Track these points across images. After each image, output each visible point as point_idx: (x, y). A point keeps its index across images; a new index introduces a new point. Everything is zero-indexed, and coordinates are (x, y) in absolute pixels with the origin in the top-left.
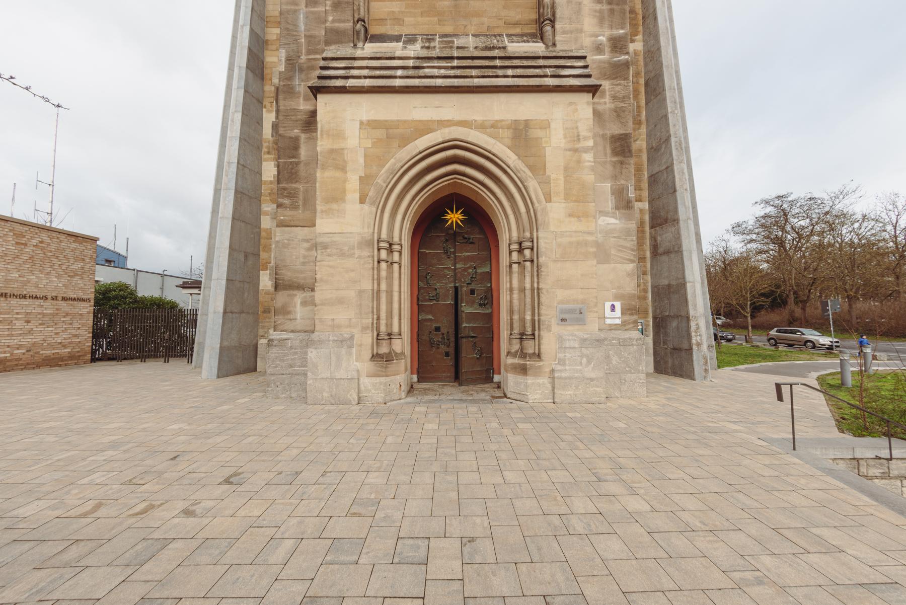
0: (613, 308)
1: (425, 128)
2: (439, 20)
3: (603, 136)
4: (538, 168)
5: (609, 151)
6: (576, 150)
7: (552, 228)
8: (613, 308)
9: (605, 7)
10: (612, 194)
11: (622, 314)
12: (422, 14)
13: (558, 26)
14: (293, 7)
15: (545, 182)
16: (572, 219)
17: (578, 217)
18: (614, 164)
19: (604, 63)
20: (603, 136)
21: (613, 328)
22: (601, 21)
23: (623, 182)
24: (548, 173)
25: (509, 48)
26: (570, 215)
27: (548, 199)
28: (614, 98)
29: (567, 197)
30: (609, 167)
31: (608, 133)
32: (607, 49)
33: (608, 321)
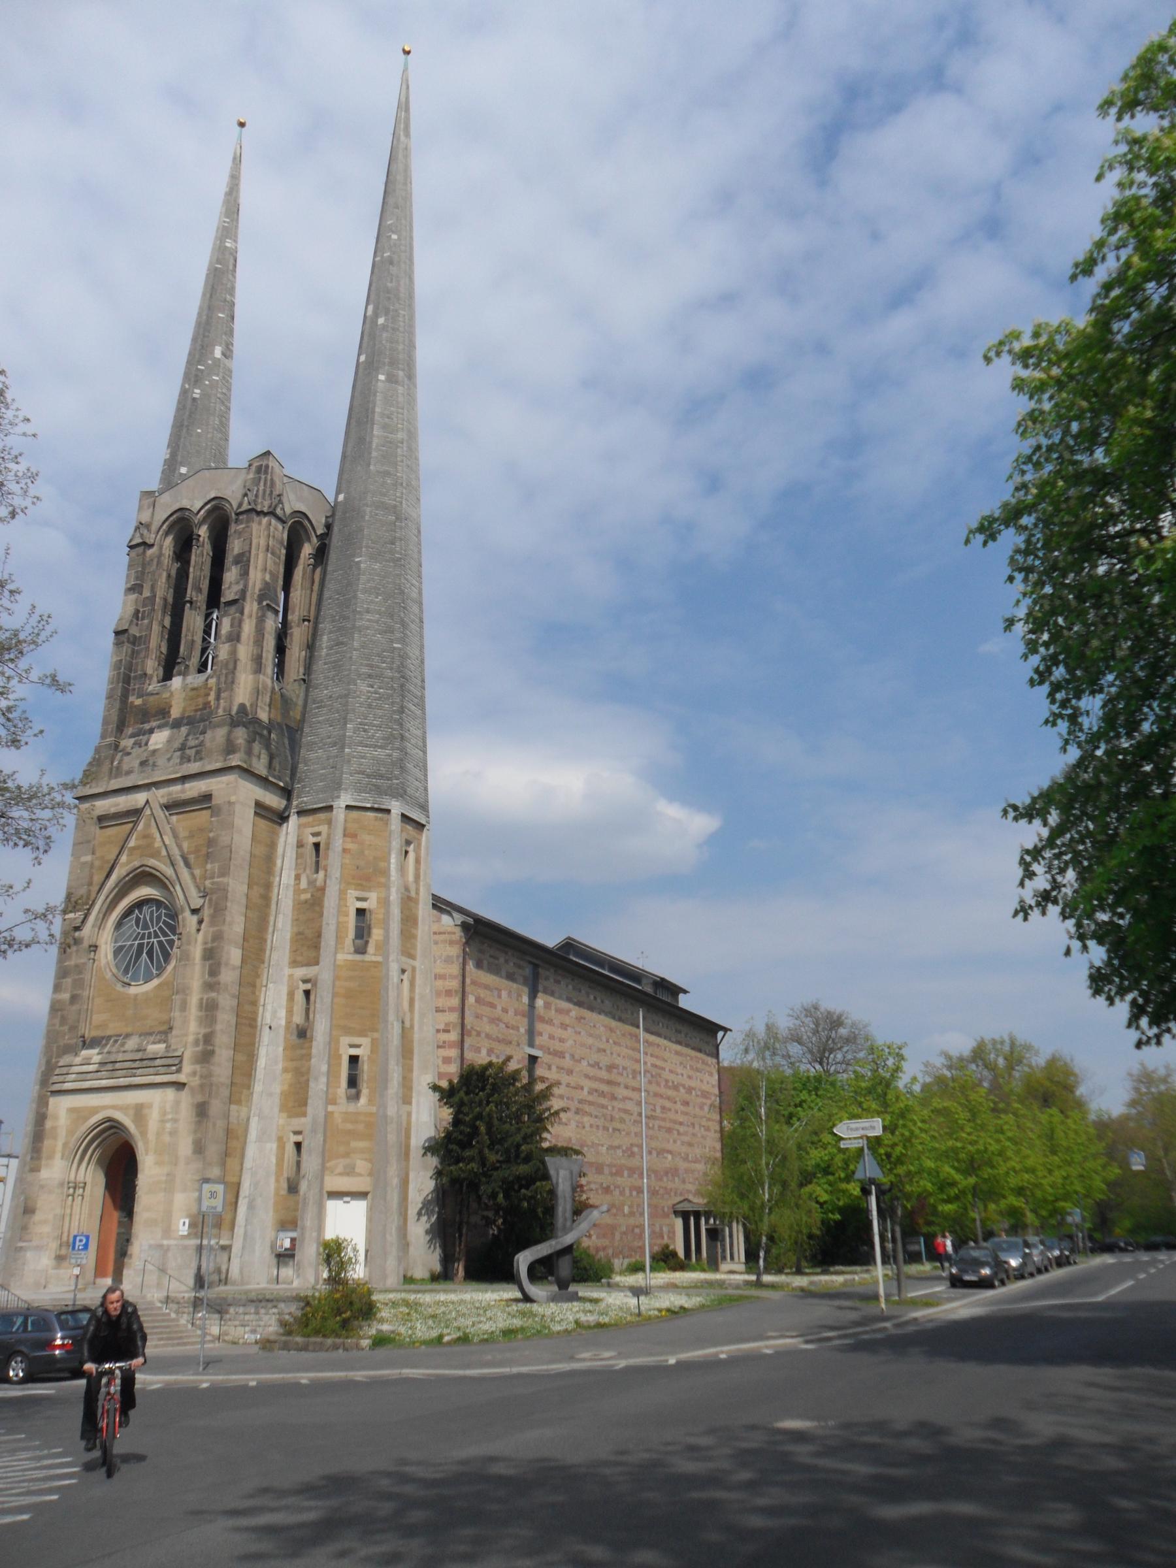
0: (184, 1223)
1: (95, 1110)
4: (144, 1134)
5: (194, 1114)
8: (184, 1223)
9: (203, 1013)
15: (146, 1142)
26: (156, 1163)
27: (147, 1154)
32: (201, 1043)
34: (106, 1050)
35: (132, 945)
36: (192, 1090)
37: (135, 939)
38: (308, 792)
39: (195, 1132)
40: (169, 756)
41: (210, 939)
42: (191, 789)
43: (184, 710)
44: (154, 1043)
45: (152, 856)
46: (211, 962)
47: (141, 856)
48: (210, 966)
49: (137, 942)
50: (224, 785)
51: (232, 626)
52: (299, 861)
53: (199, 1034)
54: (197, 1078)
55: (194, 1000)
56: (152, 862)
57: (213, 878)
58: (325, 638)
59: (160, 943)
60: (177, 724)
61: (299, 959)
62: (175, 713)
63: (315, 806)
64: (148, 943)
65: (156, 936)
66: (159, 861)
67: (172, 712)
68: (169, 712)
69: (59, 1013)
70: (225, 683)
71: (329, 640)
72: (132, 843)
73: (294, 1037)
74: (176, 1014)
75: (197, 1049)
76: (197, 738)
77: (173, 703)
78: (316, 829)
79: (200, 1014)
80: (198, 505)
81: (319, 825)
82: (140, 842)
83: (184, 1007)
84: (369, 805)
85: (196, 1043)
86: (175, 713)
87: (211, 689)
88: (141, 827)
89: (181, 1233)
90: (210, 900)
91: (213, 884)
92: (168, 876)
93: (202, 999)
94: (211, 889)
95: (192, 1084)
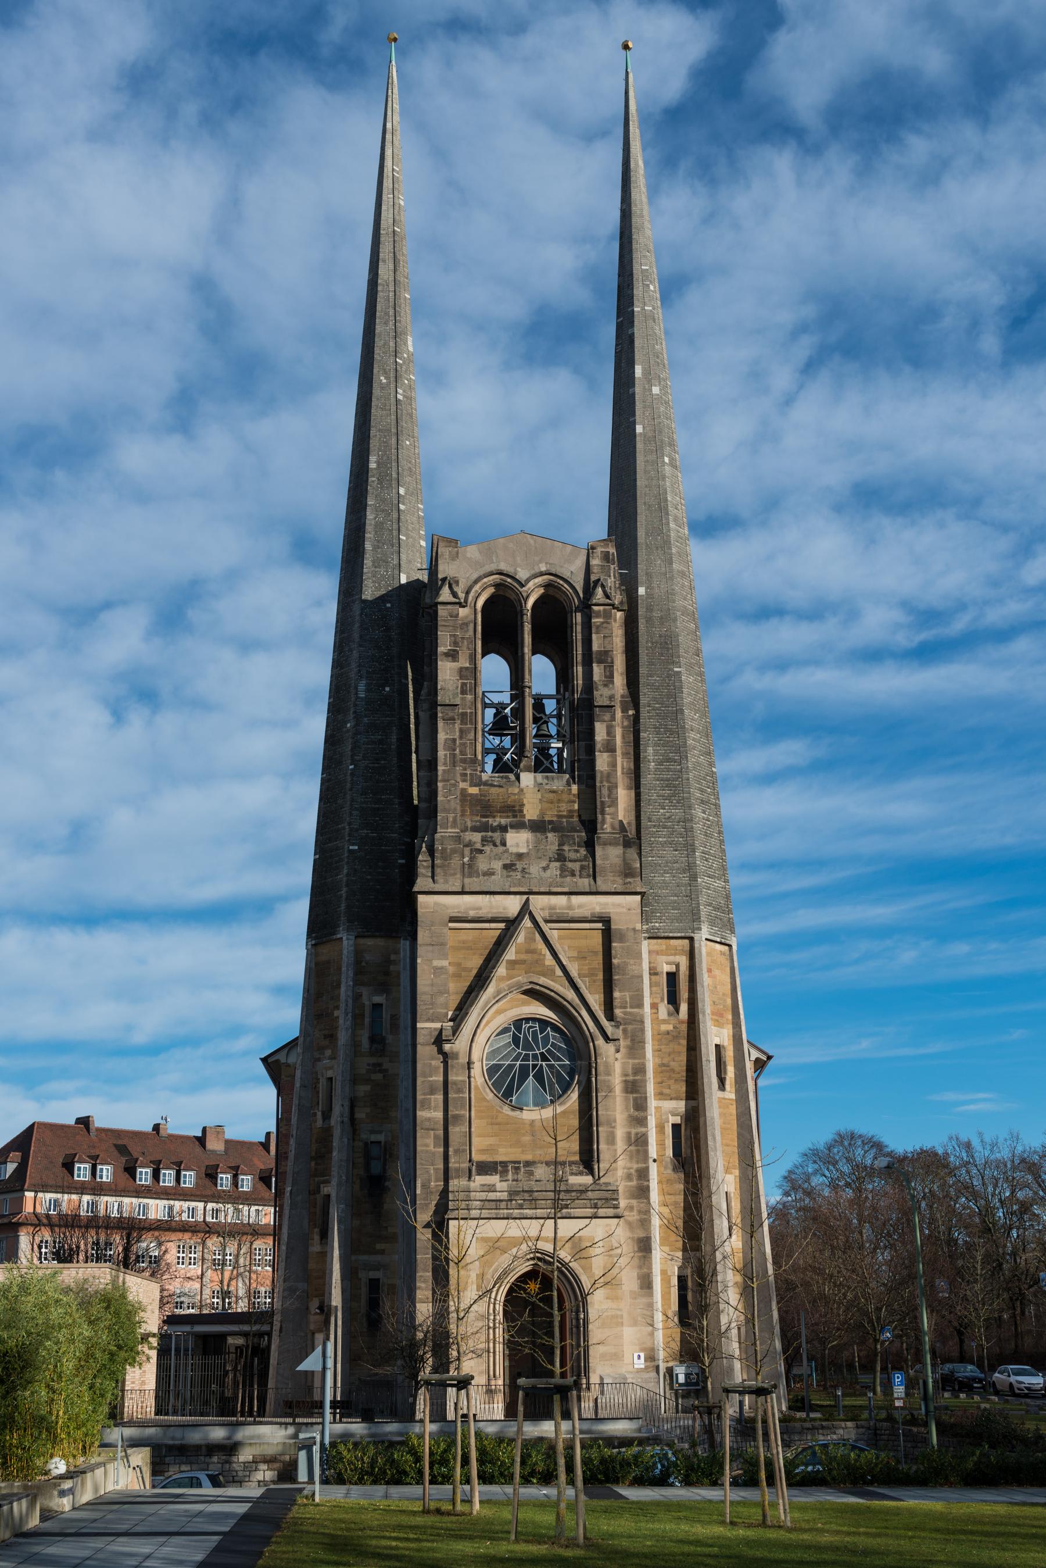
0: (639, 1356)
2: (523, 1151)
3: (633, 1239)
7: (596, 1307)
8: (639, 1356)
10: (638, 1279)
12: (511, 1146)
14: (425, 1148)
16: (609, 1301)
17: (612, 1299)
18: (640, 1258)
19: (633, 1187)
20: (633, 1239)
21: (639, 1371)
22: (631, 1158)
23: (645, 1270)
24: (594, 1270)
25: (570, 1181)
26: (607, 1298)
28: (640, 1212)
30: (636, 1260)
31: (636, 1236)
33: (636, 1366)
34: (510, 1176)
35: (511, 1067)
36: (629, 1224)
37: (516, 1059)
39: (640, 1267)
41: (630, 1071)
42: (580, 906)
43: (542, 813)
44: (572, 1174)
45: (544, 975)
48: (635, 1099)
49: (518, 1063)
50: (625, 910)
53: (629, 1169)
54: (635, 1213)
55: (620, 1133)
56: (542, 980)
57: (625, 1007)
58: (650, 750)
59: (551, 1067)
60: (538, 827)
61: (666, 1091)
62: (531, 813)
63: (671, 935)
64: (534, 1066)
65: (544, 1058)
66: (552, 981)
67: (525, 812)
68: (521, 811)
69: (432, 1132)
70: (609, 797)
71: (656, 753)
73: (670, 1171)
74: (602, 1146)
75: (631, 1184)
76: (577, 851)
77: (525, 801)
78: (671, 958)
81: (675, 955)
82: (523, 957)
83: (611, 1140)
84: (718, 940)
85: (629, 1177)
86: (531, 813)
90: (625, 1031)
91: (625, 1013)
92: (569, 999)
93: (629, 1133)
94: (624, 1019)
95: (630, 1219)
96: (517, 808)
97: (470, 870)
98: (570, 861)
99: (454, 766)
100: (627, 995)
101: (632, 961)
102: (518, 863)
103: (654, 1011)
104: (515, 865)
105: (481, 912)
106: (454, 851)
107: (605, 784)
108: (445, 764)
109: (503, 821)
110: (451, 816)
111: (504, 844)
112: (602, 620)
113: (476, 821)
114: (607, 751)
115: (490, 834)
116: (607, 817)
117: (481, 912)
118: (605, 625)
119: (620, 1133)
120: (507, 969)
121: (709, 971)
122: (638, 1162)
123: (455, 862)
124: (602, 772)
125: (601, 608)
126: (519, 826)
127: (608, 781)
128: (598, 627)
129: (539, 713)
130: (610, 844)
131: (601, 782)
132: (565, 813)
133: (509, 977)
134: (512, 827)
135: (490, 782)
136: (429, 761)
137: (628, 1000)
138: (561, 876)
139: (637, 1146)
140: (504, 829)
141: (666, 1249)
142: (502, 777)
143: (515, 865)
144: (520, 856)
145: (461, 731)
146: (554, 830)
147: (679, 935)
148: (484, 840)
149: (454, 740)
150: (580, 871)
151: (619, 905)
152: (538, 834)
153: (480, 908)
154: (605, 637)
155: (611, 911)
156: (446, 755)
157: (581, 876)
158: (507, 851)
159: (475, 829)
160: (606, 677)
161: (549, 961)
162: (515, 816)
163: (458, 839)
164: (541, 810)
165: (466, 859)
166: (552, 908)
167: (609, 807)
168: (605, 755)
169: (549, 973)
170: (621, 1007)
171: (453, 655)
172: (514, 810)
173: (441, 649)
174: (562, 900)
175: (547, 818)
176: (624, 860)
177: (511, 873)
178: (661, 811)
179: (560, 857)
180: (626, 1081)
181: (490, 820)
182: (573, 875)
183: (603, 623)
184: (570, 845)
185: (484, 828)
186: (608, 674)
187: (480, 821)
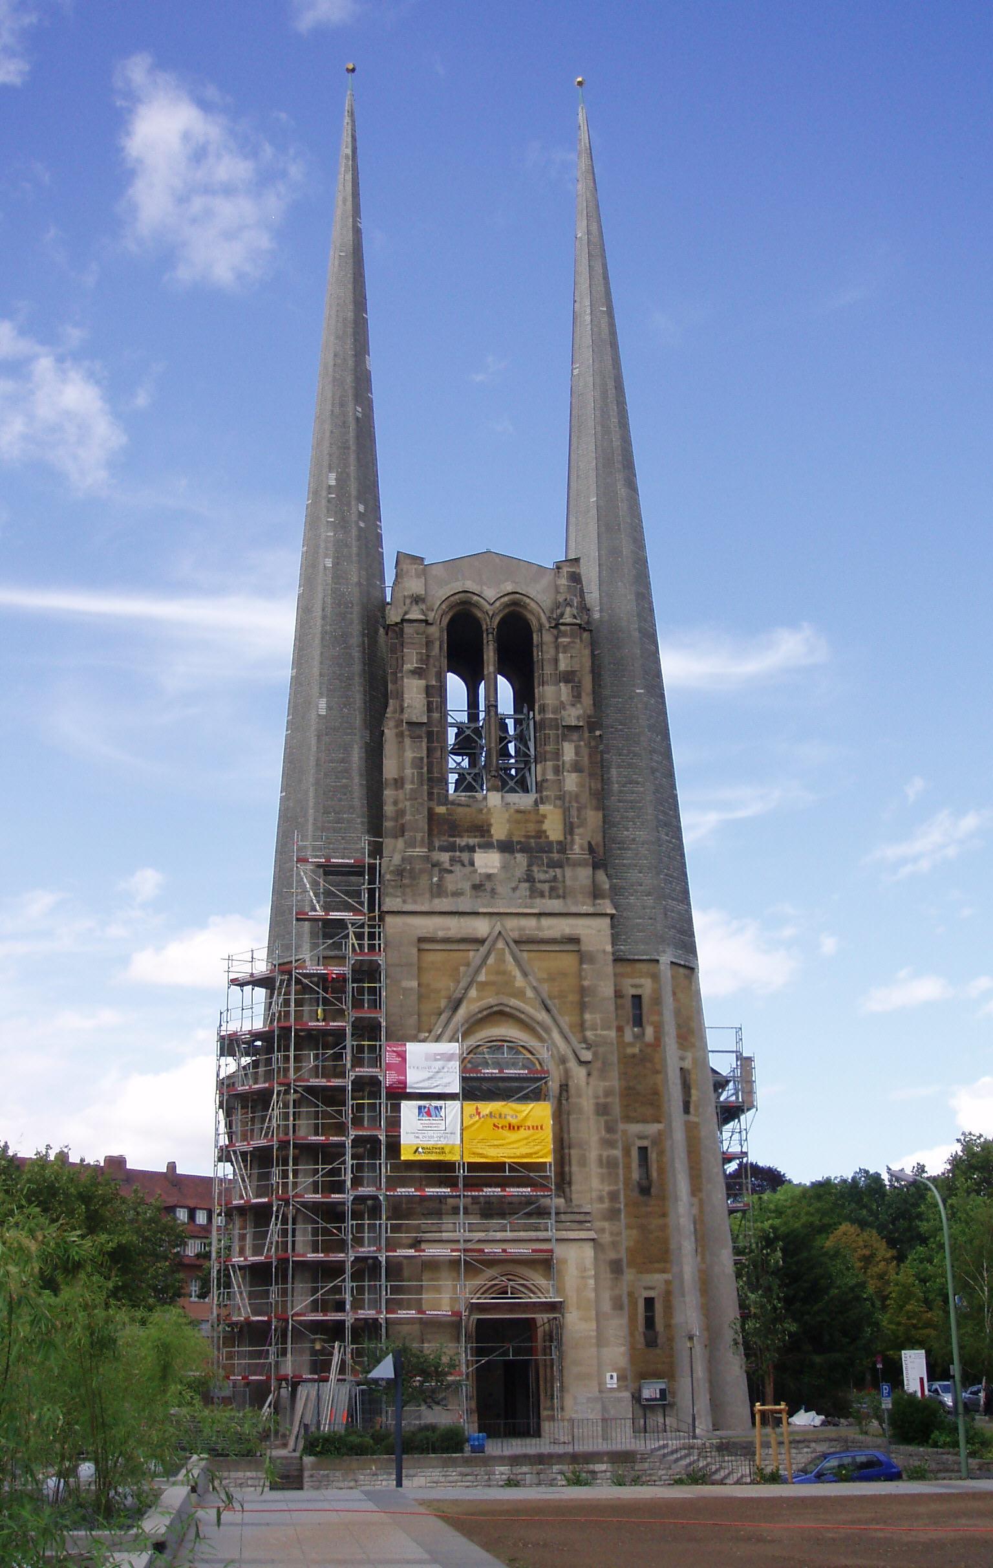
0: (612, 1376)
6: (583, 1277)
8: (612, 1376)
9: (604, 1170)
10: (611, 1299)
11: (618, 1380)
13: (573, 1188)
22: (602, 1181)
28: (612, 1234)
29: (578, 1308)
32: (606, 1200)
38: (625, 940)
40: (513, 885)
41: (601, 1093)
42: (549, 928)
43: (510, 834)
46: (605, 1117)
47: (497, 994)
48: (606, 1122)
51: (577, 754)
52: (620, 1012)
53: (600, 1191)
55: (593, 1154)
56: (513, 1002)
57: (596, 1030)
63: (636, 957)
68: (489, 831)
72: (482, 977)
74: (575, 1168)
76: (546, 872)
77: (493, 821)
79: (599, 1170)
80: (490, 593)
81: (640, 977)
82: (492, 978)
83: (583, 1163)
84: (682, 963)
86: (499, 832)
87: (544, 816)
88: (491, 961)
89: (609, 1386)
90: (595, 1054)
91: (596, 1035)
93: (601, 1156)
96: (485, 828)
97: (439, 891)
98: (539, 882)
99: (422, 785)
100: (598, 1016)
101: (602, 983)
102: (487, 883)
103: (620, 1033)
104: (484, 885)
105: (449, 933)
106: (422, 871)
107: (575, 805)
108: (412, 782)
109: (472, 841)
110: (419, 836)
111: (472, 864)
112: (568, 640)
113: (444, 841)
114: (576, 772)
115: (458, 854)
116: (576, 838)
117: (449, 933)
118: (572, 645)
119: (593, 1154)
120: (477, 990)
121: (674, 994)
122: (609, 1185)
123: (424, 882)
124: (570, 792)
125: (568, 628)
126: (487, 846)
127: (577, 802)
128: (565, 647)
129: (503, 733)
130: (580, 865)
131: (570, 802)
132: (533, 834)
133: (480, 999)
134: (480, 847)
135: (457, 802)
136: (395, 780)
137: (599, 1021)
138: (531, 897)
139: (608, 1168)
140: (471, 849)
141: (633, 1271)
142: (469, 797)
143: (484, 885)
144: (489, 876)
145: (428, 749)
146: (522, 851)
147: (645, 957)
148: (453, 860)
149: (423, 758)
150: (550, 892)
151: (589, 927)
152: (507, 855)
153: (449, 929)
154: (571, 656)
155: (581, 932)
156: (413, 773)
157: (550, 898)
158: (475, 871)
159: (443, 849)
160: (573, 697)
161: (520, 982)
162: (483, 836)
163: (427, 858)
164: (509, 830)
165: (435, 879)
166: (522, 929)
167: (578, 827)
168: (574, 775)
169: (520, 994)
170: (592, 1029)
171: (418, 673)
172: (482, 830)
173: (408, 667)
174: (532, 922)
175: (515, 839)
176: (594, 881)
177: (480, 894)
178: (625, 833)
179: (530, 879)
180: (597, 1104)
181: (458, 840)
182: (542, 895)
183: (569, 643)
184: (539, 866)
185: (451, 848)
186: (575, 694)
187: (447, 841)
